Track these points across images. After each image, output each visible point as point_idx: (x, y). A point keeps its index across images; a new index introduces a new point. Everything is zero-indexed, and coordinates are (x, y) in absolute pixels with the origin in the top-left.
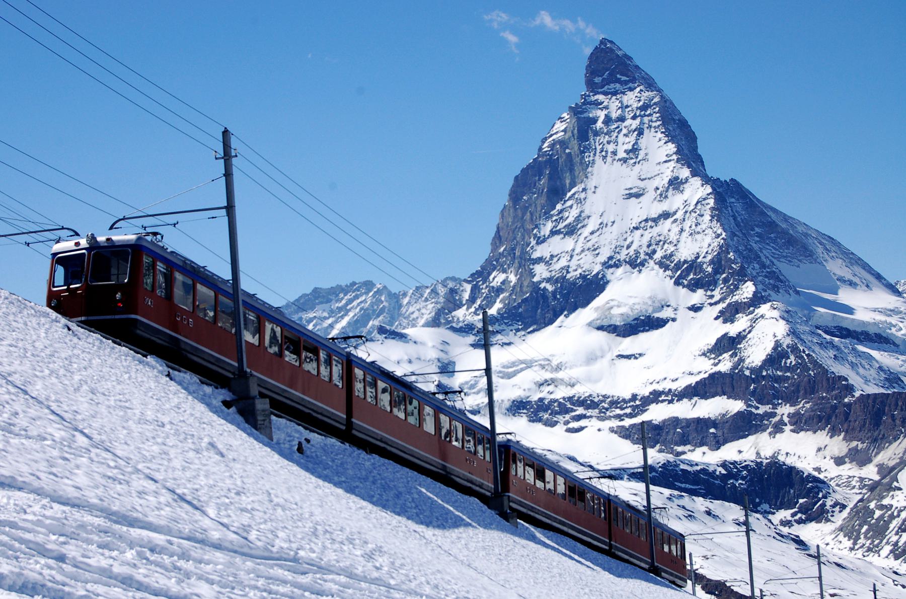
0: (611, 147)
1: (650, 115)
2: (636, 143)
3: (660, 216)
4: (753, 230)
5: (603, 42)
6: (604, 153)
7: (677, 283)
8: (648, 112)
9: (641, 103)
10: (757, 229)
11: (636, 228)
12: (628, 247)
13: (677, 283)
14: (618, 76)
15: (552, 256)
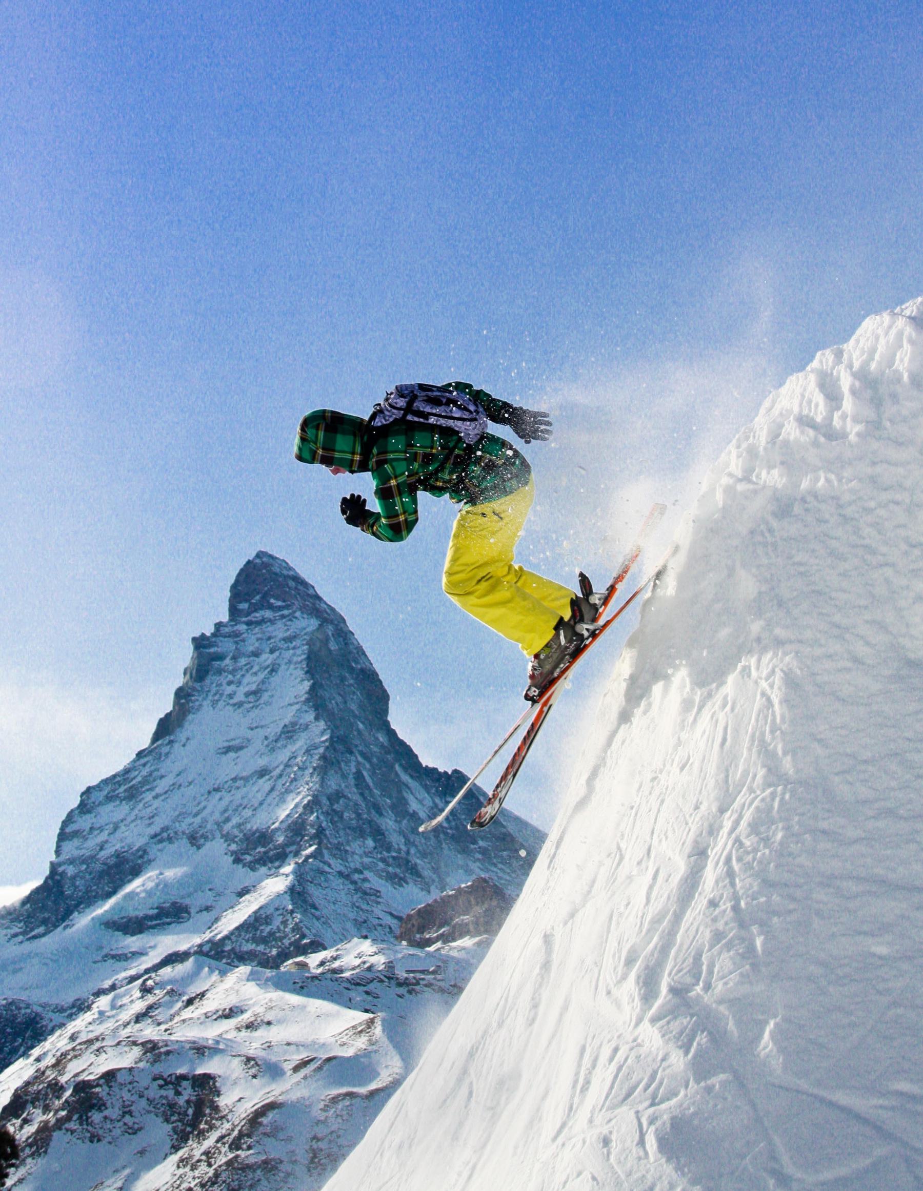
0: (229, 689)
1: (294, 648)
2: (263, 682)
3: (252, 776)
4: (474, 842)
5: (260, 555)
6: (216, 698)
7: (237, 861)
8: (291, 645)
9: (288, 633)
10: (481, 843)
11: (217, 790)
12: (196, 815)
13: (237, 861)
14: (272, 601)
15: (91, 828)
